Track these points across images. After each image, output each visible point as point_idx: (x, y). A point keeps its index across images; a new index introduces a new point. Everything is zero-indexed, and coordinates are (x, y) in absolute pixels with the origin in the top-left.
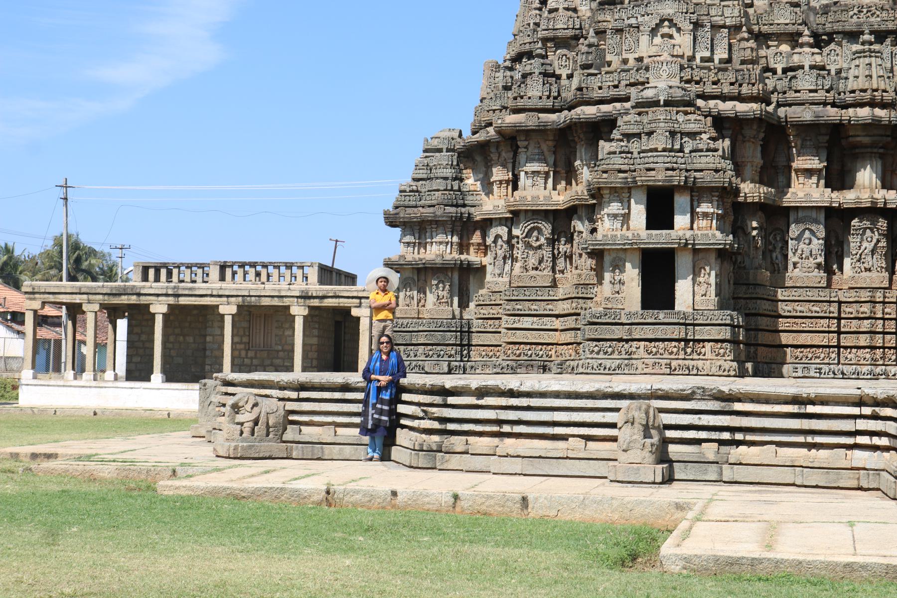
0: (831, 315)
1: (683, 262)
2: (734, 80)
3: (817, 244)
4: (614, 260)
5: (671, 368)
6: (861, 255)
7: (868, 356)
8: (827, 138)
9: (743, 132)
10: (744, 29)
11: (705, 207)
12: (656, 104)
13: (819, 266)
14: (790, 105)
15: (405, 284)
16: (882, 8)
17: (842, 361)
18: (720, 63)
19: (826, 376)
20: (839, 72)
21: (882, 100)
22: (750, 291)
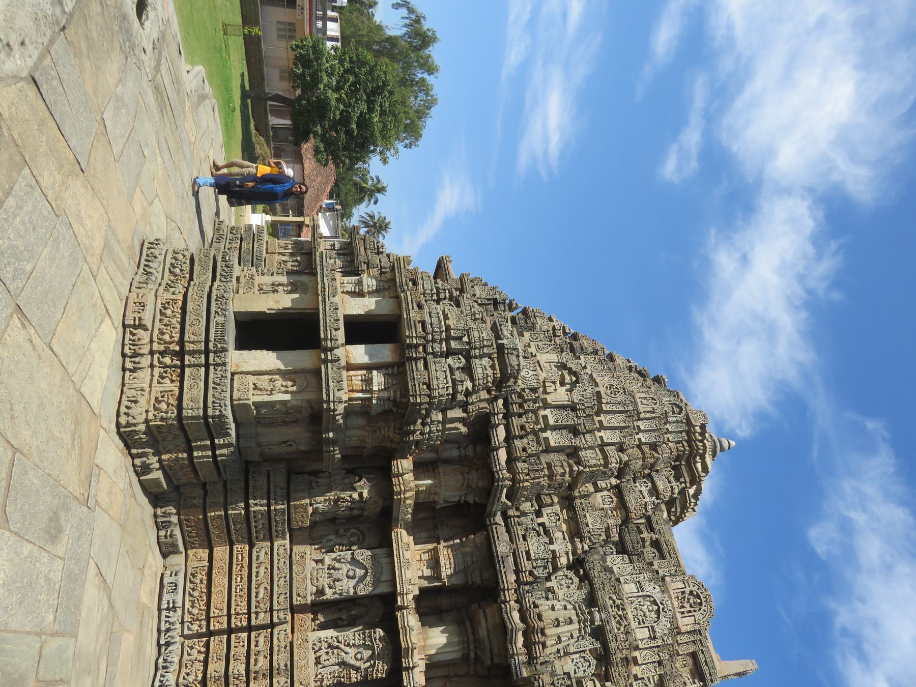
0: (253, 616)
1: (303, 358)
2: (529, 451)
3: (347, 587)
4: (304, 284)
5: (135, 327)
6: (337, 648)
7: (191, 678)
8: (478, 581)
9: (474, 471)
10: (581, 468)
11: (378, 379)
12: (498, 337)
13: (320, 592)
14: (508, 531)
15: (297, 244)
16: (628, 632)
17: (187, 642)
18: (544, 438)
19: (163, 618)
20: (550, 590)
21: (534, 643)
22: (279, 492)
